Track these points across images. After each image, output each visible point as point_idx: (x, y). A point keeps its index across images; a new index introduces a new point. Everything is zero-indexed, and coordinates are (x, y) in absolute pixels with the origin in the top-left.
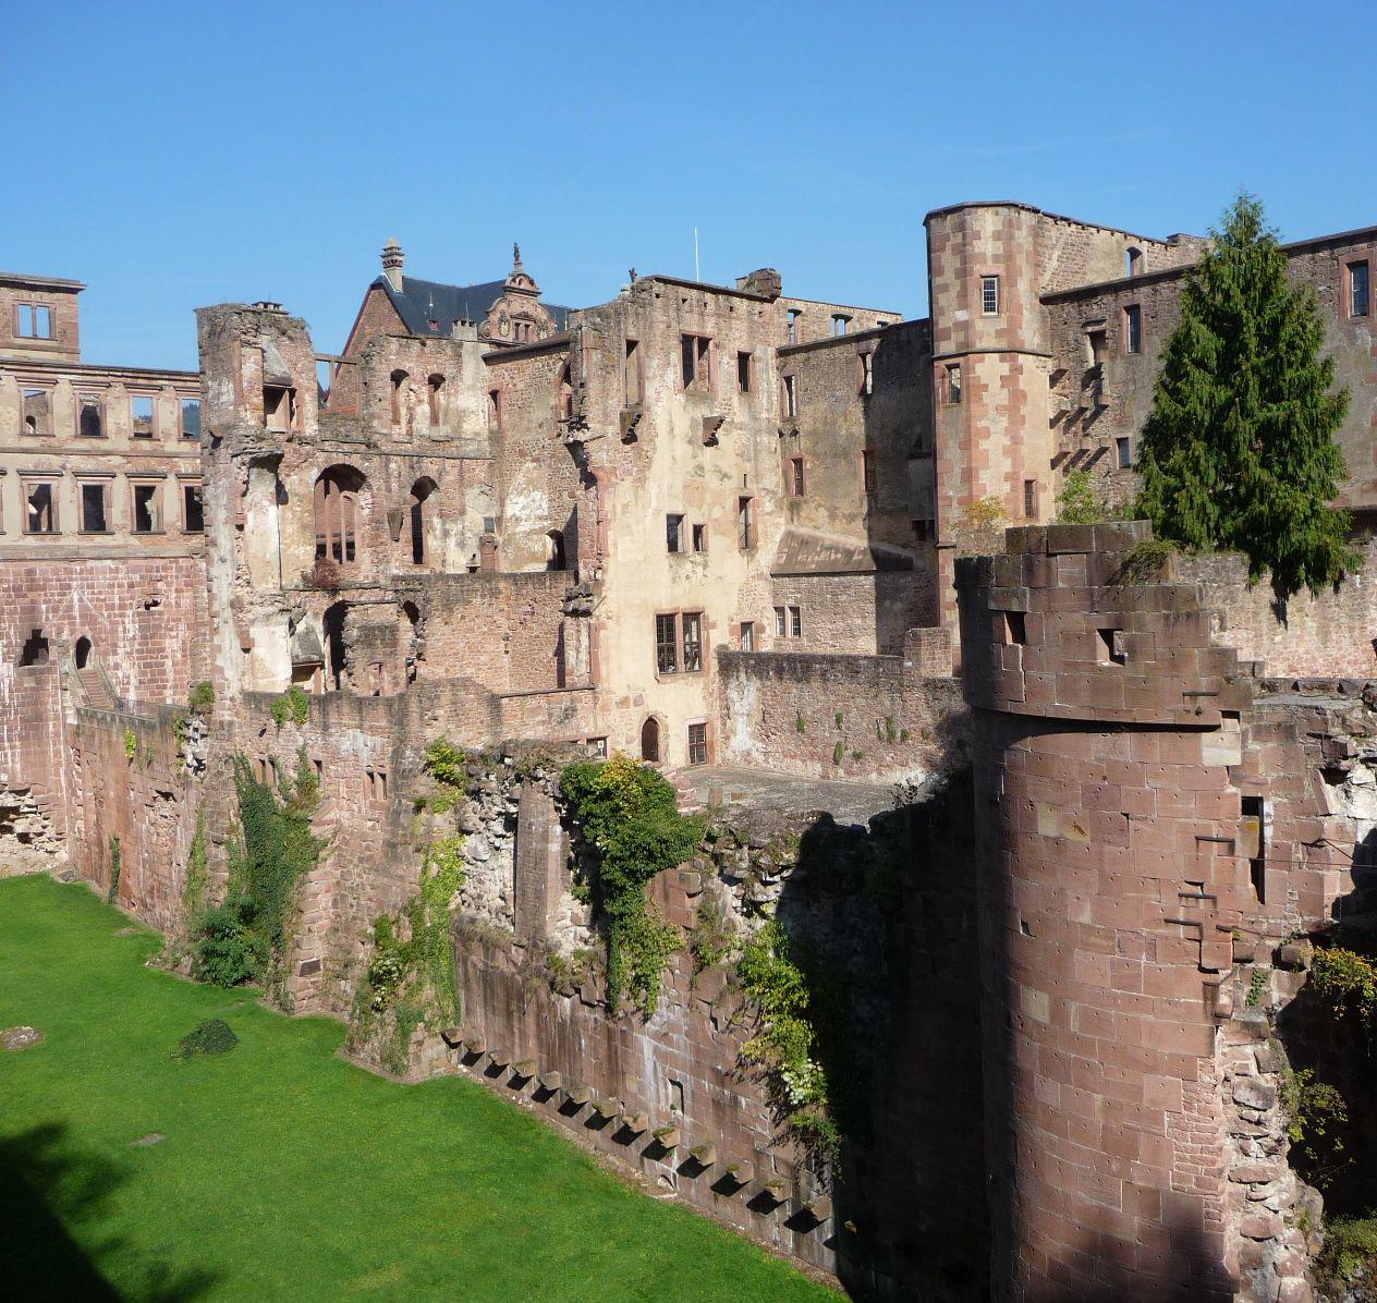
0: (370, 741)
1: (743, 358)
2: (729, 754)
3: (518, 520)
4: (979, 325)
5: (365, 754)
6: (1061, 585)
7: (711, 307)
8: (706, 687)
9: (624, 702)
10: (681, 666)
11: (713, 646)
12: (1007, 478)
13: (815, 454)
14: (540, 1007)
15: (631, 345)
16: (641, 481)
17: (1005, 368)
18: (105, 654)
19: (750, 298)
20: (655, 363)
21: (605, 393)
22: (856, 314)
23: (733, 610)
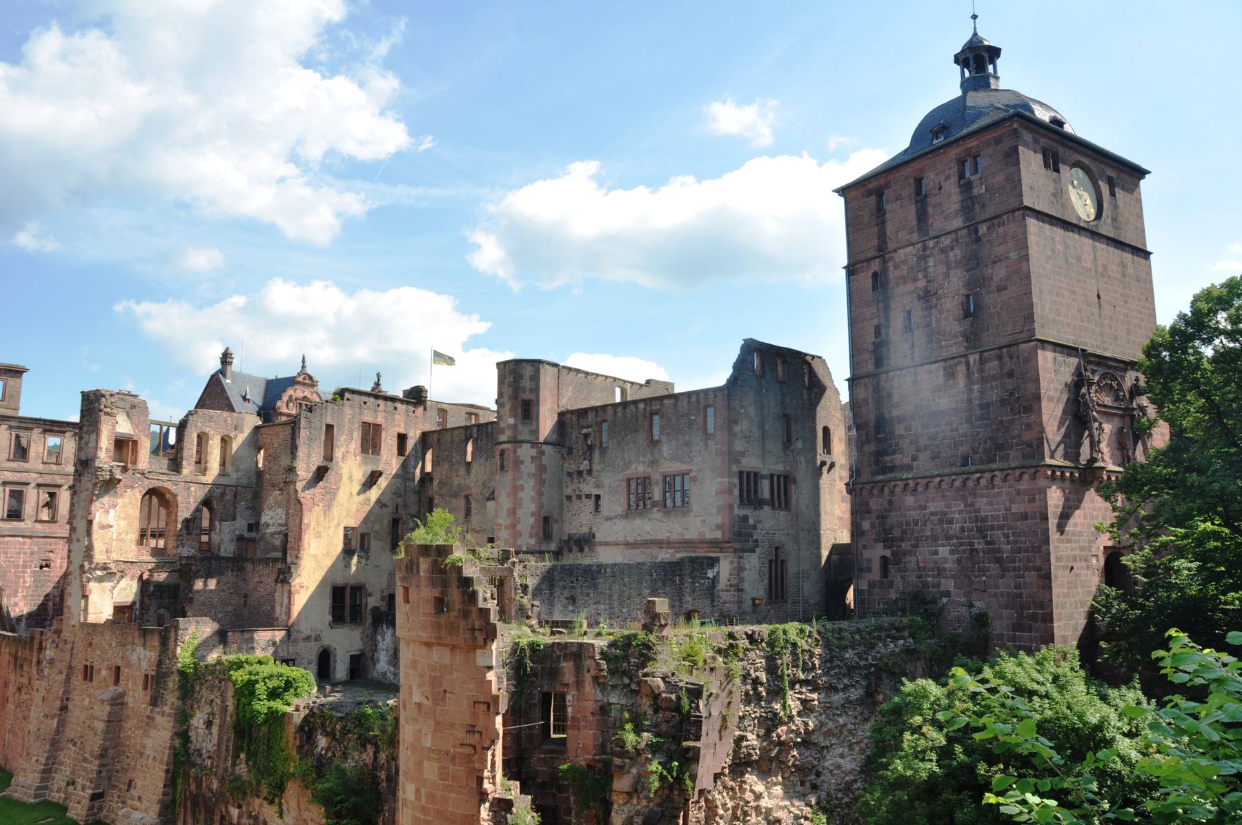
0: (148, 653)
1: (402, 438)
2: (375, 674)
3: (268, 525)
4: (520, 427)
5: (144, 665)
6: (422, 574)
7: (382, 407)
8: (363, 633)
9: (308, 638)
10: (348, 619)
11: (369, 607)
12: (532, 514)
13: (441, 496)
14: (223, 818)
15: (330, 428)
16: (329, 506)
17: (534, 452)
18: (9, 596)
19: (408, 403)
20: (343, 438)
21: (309, 456)
22: (481, 412)
23: (384, 586)
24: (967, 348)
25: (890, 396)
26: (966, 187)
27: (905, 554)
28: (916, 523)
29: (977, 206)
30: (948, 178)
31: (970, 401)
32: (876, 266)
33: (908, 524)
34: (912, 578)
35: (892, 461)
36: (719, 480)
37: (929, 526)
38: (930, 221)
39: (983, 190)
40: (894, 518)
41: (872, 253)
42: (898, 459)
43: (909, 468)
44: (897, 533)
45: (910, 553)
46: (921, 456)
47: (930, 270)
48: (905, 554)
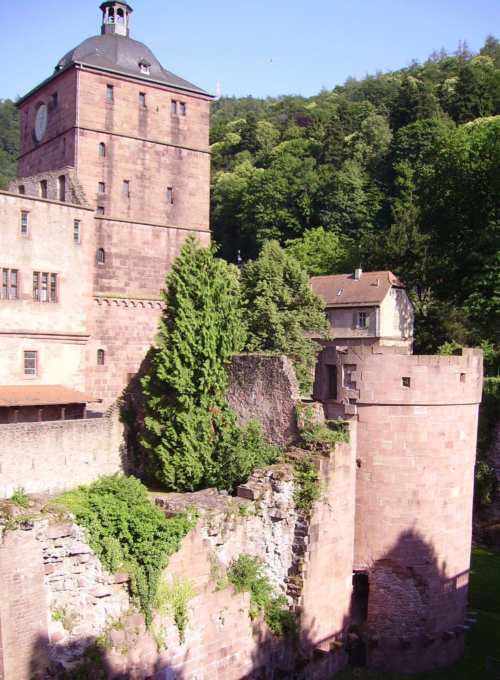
24: (168, 223)
25: (110, 237)
26: (176, 120)
27: (118, 348)
28: (127, 328)
29: (181, 136)
30: (164, 107)
31: (168, 256)
32: (104, 138)
33: (120, 328)
34: (123, 365)
35: (109, 283)
36: (86, 284)
37: (135, 332)
38: (149, 128)
39: (186, 128)
40: (109, 324)
41: (100, 127)
42: (113, 283)
43: (123, 290)
44: (112, 334)
45: (121, 348)
46: (132, 283)
47: (147, 162)
48: (118, 348)
